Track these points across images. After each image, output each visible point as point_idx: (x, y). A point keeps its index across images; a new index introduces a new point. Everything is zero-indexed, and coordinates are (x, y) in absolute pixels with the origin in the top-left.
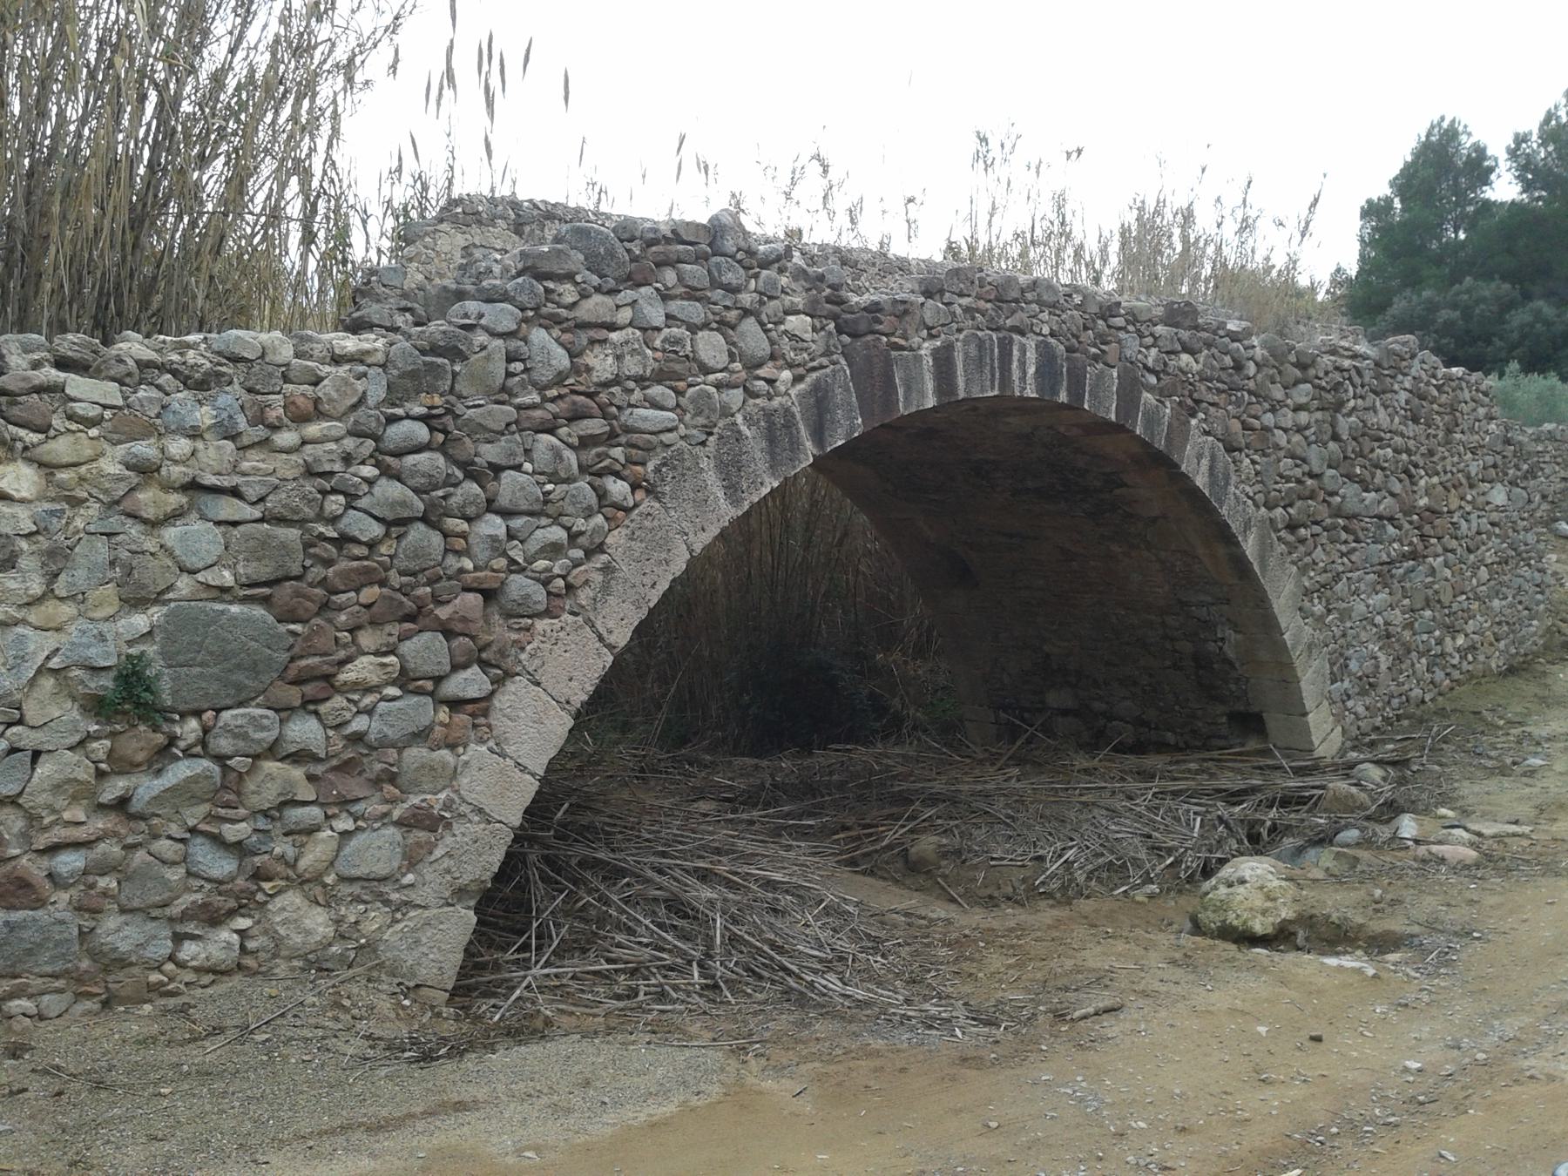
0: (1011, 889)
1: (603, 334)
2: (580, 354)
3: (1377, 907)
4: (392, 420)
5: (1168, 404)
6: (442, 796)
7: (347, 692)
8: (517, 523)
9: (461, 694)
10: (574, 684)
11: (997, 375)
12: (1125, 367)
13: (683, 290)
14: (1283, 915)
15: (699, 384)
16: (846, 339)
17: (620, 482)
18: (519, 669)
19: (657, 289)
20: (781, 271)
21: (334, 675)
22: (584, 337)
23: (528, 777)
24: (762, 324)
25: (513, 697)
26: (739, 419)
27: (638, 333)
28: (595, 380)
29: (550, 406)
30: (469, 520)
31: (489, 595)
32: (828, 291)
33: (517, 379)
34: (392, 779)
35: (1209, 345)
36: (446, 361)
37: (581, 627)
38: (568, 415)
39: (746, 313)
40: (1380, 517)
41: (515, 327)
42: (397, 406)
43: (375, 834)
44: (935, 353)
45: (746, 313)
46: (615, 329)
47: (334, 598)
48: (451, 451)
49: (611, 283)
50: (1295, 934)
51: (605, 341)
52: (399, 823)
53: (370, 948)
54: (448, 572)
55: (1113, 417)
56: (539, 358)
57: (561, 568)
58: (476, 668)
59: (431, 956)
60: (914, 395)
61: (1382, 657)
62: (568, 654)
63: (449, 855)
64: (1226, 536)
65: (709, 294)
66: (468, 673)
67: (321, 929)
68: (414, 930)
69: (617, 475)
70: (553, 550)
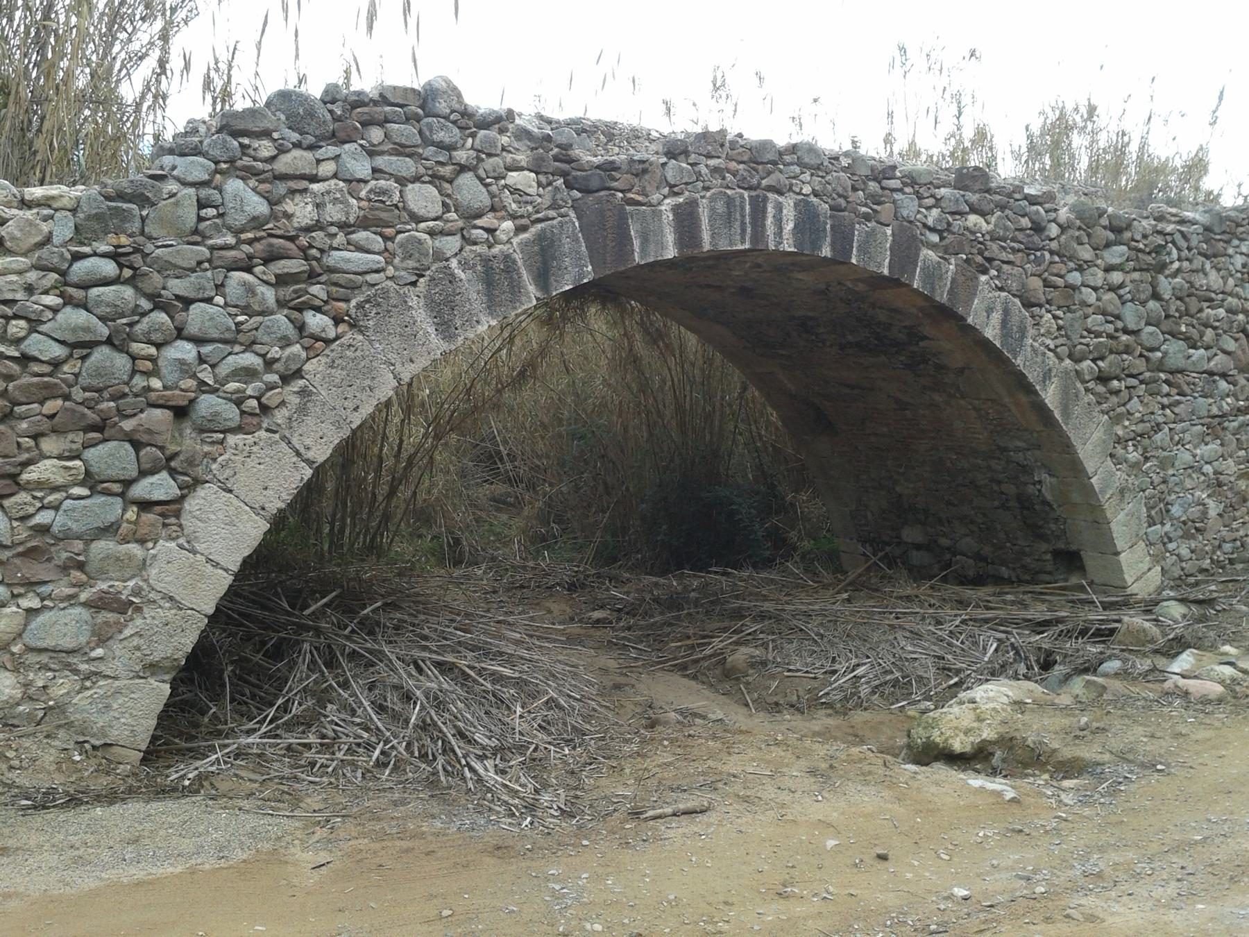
0: (795, 698)
1: (304, 184)
2: (278, 202)
3: (1078, 736)
4: (77, 257)
5: (953, 261)
6: (131, 584)
7: (33, 490)
8: (207, 349)
9: (147, 497)
10: (269, 492)
11: (749, 230)
12: (901, 226)
13: (392, 146)
14: (984, 736)
15: (409, 231)
16: (576, 194)
17: (319, 316)
18: (209, 477)
19: (361, 146)
20: (502, 131)
21: (19, 474)
22: (282, 188)
23: (220, 571)
24: (481, 180)
25: (202, 501)
26: (454, 263)
27: (341, 184)
28: (296, 225)
29: (246, 248)
30: (158, 346)
31: (181, 413)
32: (556, 150)
33: (208, 223)
34: (81, 566)
35: (1003, 208)
36: (134, 206)
37: (276, 443)
38: (263, 255)
39: (462, 168)
40: (1211, 374)
41: (206, 177)
42: (85, 245)
43: (62, 612)
44: (676, 209)
45: (462, 168)
46: (318, 181)
47: (16, 408)
48: (140, 285)
49: (310, 139)
50: (992, 754)
51: (305, 190)
52: (85, 604)
53: (60, 708)
54: (134, 390)
55: (886, 272)
56: (231, 205)
57: (254, 389)
58: (164, 474)
59: (123, 720)
60: (652, 246)
61: (1211, 504)
62: (262, 467)
63: (138, 634)
64: (1021, 384)
65: (421, 151)
66: (154, 479)
67: (7, 691)
68: (106, 697)
69: (318, 309)
70: (248, 374)
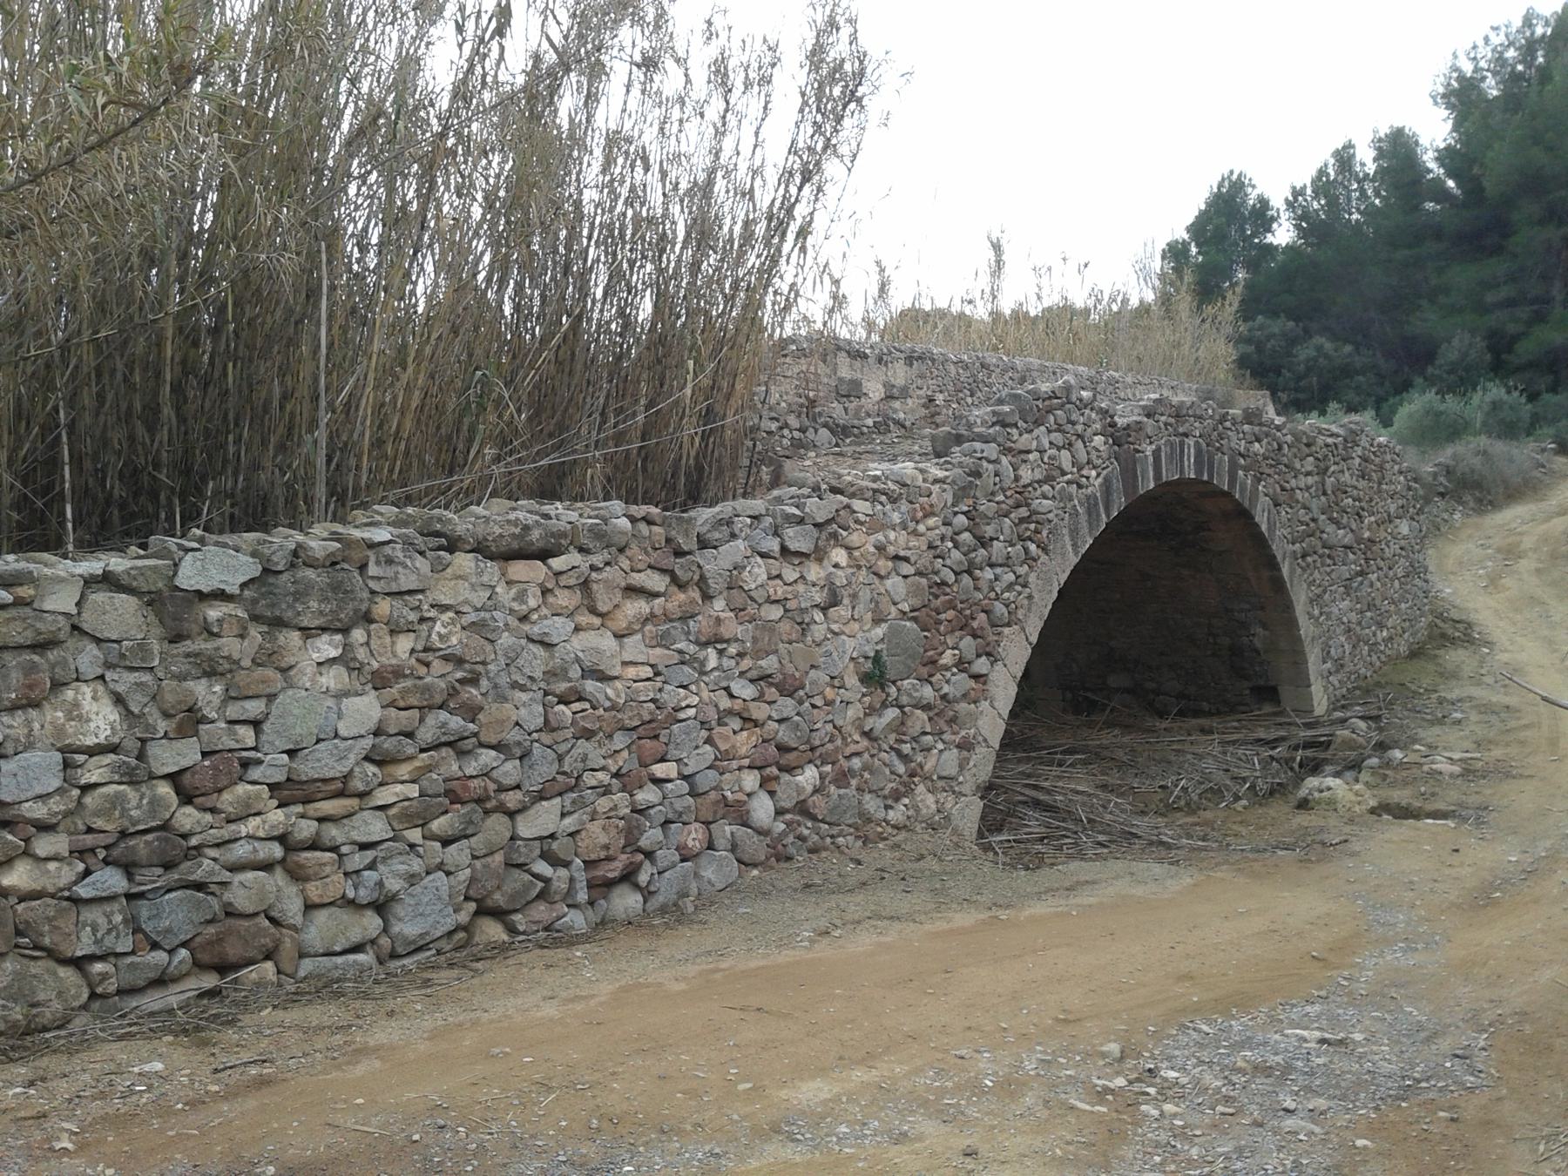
16: (1116, 448)
35: (1267, 435)
40: (1346, 547)
55: (1226, 488)
61: (1347, 646)
64: (1273, 564)
